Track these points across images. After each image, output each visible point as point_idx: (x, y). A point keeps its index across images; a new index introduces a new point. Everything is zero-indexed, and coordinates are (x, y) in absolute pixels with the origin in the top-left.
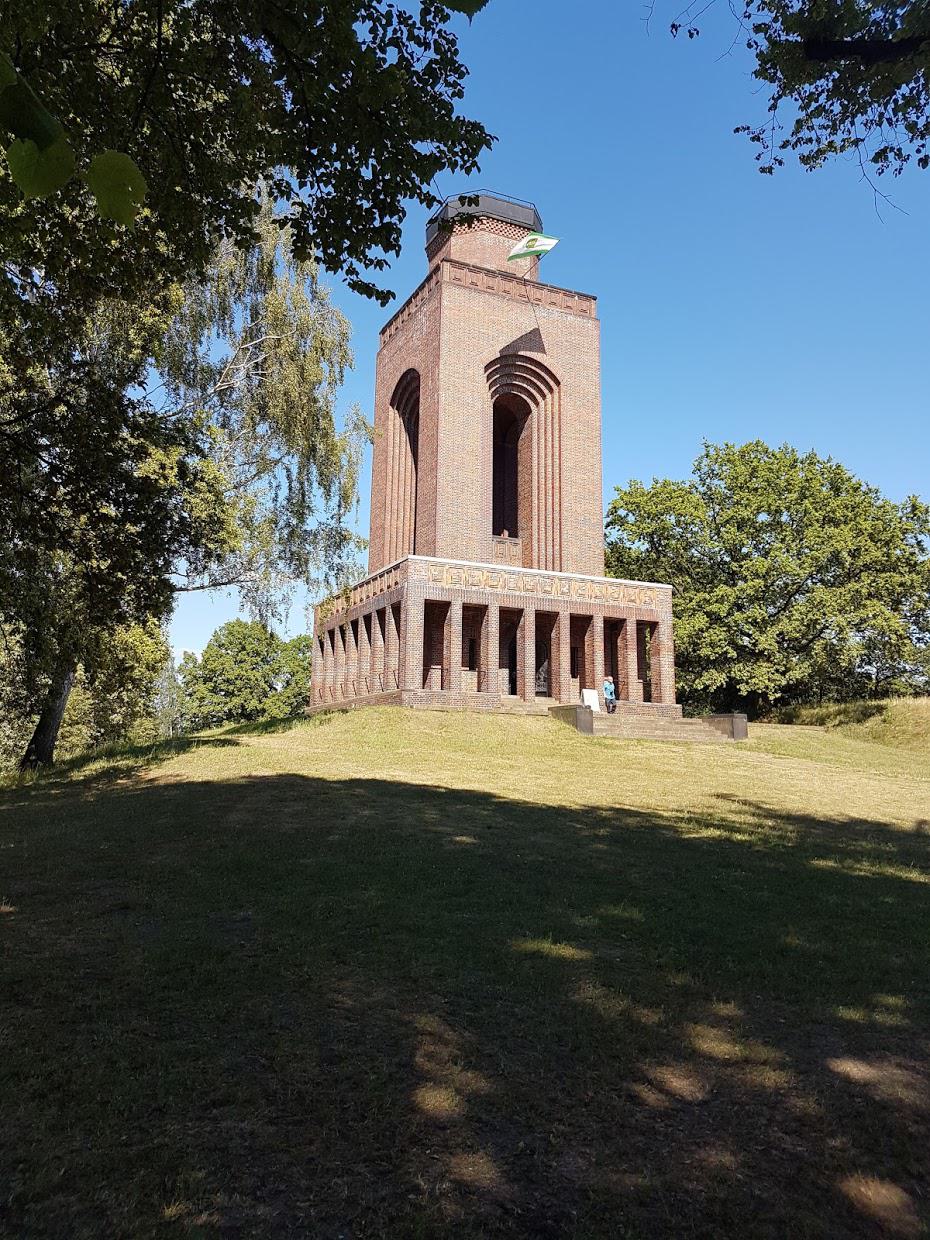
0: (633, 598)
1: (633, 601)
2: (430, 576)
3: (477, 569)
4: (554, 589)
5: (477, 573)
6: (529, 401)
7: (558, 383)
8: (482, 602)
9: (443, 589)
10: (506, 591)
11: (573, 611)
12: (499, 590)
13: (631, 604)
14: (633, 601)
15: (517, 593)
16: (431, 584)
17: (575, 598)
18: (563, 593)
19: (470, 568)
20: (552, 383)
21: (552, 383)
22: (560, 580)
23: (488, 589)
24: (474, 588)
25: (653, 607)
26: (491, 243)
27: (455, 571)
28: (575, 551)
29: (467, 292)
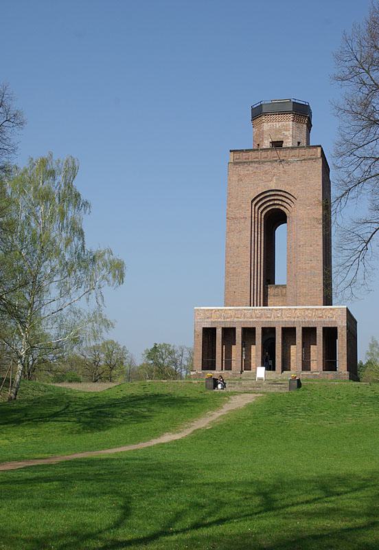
10: (246, 319)
13: (319, 319)
15: (251, 320)
18: (278, 317)
22: (276, 310)
24: (228, 320)
25: (334, 319)
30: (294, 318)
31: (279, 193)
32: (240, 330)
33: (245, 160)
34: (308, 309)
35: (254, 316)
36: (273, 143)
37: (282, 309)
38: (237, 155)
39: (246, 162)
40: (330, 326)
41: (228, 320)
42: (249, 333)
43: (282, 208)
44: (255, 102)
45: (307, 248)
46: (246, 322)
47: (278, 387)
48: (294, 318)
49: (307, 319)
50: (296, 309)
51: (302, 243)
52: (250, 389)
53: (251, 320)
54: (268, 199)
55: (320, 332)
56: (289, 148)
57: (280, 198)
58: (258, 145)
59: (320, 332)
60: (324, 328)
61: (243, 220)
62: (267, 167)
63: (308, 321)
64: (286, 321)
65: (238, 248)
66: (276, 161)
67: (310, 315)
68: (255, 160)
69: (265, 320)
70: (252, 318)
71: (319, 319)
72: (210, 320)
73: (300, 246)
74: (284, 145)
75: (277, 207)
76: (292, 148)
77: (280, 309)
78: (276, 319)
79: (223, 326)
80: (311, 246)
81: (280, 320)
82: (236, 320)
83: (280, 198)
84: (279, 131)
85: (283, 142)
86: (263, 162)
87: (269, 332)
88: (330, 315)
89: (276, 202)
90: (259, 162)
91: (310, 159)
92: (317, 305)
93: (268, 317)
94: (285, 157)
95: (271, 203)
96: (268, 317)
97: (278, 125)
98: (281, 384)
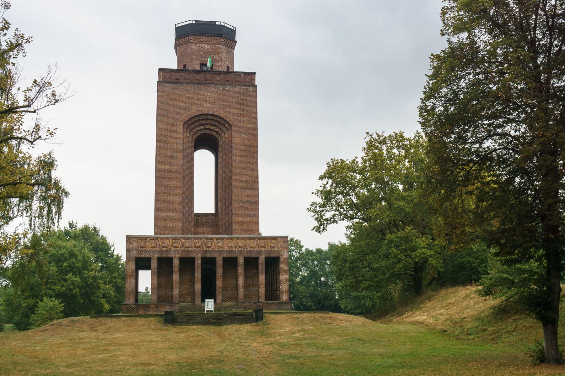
0: (263, 245)
1: (263, 247)
3: (167, 238)
5: (167, 242)
6: (217, 136)
7: (230, 125)
8: (168, 256)
9: (146, 251)
10: (183, 249)
11: (225, 256)
13: (261, 249)
14: (263, 247)
15: (190, 249)
16: (140, 249)
17: (226, 248)
18: (219, 246)
19: (162, 239)
21: (227, 126)
22: (217, 239)
23: (173, 248)
24: (164, 249)
25: (276, 249)
26: (196, 49)
27: (153, 241)
28: (240, 219)
29: (172, 85)
30: (236, 247)
31: (212, 118)
34: (250, 239)
35: (193, 244)
37: (223, 239)
40: (272, 256)
42: (187, 263)
43: (214, 134)
46: (184, 251)
48: (236, 247)
49: (249, 249)
55: (262, 262)
56: (223, 72)
59: (262, 262)
63: (250, 251)
64: (227, 251)
67: (252, 245)
69: (205, 249)
70: (192, 247)
71: (261, 249)
72: (144, 249)
75: (208, 132)
76: (196, 71)
77: (221, 238)
78: (217, 249)
81: (221, 249)
82: (173, 249)
87: (209, 263)
88: (272, 245)
89: (208, 127)
93: (208, 247)
96: (208, 247)
97: (207, 47)
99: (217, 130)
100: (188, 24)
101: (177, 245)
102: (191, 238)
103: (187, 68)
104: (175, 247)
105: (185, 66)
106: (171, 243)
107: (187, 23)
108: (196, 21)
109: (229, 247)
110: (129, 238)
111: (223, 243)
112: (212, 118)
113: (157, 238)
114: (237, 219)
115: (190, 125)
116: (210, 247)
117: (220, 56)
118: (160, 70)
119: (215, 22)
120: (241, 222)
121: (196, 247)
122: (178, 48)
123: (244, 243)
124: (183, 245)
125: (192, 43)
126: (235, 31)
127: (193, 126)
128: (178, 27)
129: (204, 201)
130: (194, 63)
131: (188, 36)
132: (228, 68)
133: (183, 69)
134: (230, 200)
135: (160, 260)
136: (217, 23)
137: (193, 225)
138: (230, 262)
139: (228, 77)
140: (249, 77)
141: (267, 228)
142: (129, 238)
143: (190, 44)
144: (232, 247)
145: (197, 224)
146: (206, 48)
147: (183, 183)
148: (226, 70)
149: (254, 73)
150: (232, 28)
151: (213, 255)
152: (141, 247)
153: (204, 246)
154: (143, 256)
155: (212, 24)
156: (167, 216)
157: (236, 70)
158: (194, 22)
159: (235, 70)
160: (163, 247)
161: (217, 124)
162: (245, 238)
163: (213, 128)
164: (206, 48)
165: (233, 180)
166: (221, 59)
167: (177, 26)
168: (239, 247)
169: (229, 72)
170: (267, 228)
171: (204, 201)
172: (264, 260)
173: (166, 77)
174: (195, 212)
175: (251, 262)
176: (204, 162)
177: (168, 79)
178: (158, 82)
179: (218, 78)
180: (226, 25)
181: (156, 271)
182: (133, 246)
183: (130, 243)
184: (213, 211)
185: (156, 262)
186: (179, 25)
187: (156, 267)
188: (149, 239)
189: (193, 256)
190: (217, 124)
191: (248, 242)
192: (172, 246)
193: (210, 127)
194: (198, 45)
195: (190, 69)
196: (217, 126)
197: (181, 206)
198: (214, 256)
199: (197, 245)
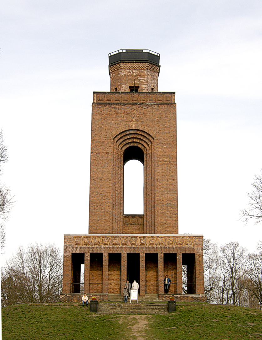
0: (180, 243)
2: (74, 242)
4: (137, 242)
5: (97, 239)
7: (153, 139)
8: (99, 252)
10: (112, 246)
11: (147, 252)
12: (108, 246)
13: (179, 246)
14: (181, 244)
15: (118, 246)
16: (75, 246)
17: (148, 246)
18: (142, 244)
20: (151, 139)
21: (151, 139)
22: (140, 237)
24: (95, 246)
27: (86, 239)
30: (156, 245)
31: (138, 132)
32: (107, 255)
33: (107, 102)
34: (169, 237)
36: (130, 87)
38: (101, 97)
39: (109, 104)
41: (95, 246)
42: (115, 259)
43: (140, 146)
44: (114, 50)
45: (164, 182)
47: (156, 309)
48: (156, 245)
49: (168, 246)
50: (158, 237)
51: (159, 178)
52: (132, 310)
53: (118, 246)
54: (128, 137)
56: (147, 93)
57: (139, 137)
58: (116, 89)
60: (183, 254)
61: (106, 155)
62: (128, 108)
64: (149, 248)
65: (101, 180)
66: (136, 103)
67: (171, 242)
68: (117, 102)
70: (118, 244)
71: (179, 246)
72: (78, 246)
73: (157, 180)
74: (140, 90)
75: (135, 145)
77: (143, 237)
79: (91, 252)
80: (167, 180)
81: (143, 246)
82: (103, 246)
83: (139, 137)
84: (136, 77)
85: (138, 87)
86: (124, 104)
87: (133, 258)
88: (188, 243)
90: (120, 104)
91: (166, 104)
92: (173, 233)
93: (133, 244)
94: (143, 100)
95: (131, 141)
96: (133, 244)
98: (158, 306)
99: (142, 142)
100: (119, 53)
101: (106, 242)
102: (118, 236)
103: (118, 91)
104: (105, 244)
105: (116, 89)
106: (101, 240)
107: (117, 52)
108: (126, 50)
109: (151, 244)
110: (66, 237)
111: (145, 240)
112: (138, 132)
113: (89, 236)
114: (160, 220)
115: (119, 139)
116: (135, 244)
117: (146, 79)
118: (94, 93)
119: (143, 50)
120: (163, 222)
121: (123, 244)
122: (111, 74)
123: (164, 241)
124: (111, 243)
125: (121, 69)
126: (159, 57)
127: (121, 140)
128: (111, 56)
129: (134, 203)
130: (124, 86)
131: (119, 63)
132: (152, 89)
133: (115, 91)
134: (153, 202)
135: (93, 255)
136: (144, 51)
137: (121, 224)
138: (152, 259)
139: (153, 97)
140: (170, 96)
141: (186, 227)
142: (66, 237)
143: (120, 71)
144: (153, 244)
145: (125, 224)
146: (134, 73)
147: (113, 189)
148: (150, 91)
149: (174, 93)
150: (157, 54)
151: (69, 256)
152: (76, 244)
153: (129, 243)
154: (78, 252)
155: (140, 52)
156: (99, 217)
157: (160, 90)
158: (125, 51)
159: (159, 91)
160: (95, 244)
161: (142, 138)
162: (165, 237)
163: (139, 141)
164: (134, 73)
165: (156, 186)
166: (147, 82)
167: (110, 55)
168: (160, 244)
169: (153, 92)
170: (186, 227)
171: (134, 203)
172: (181, 256)
173: (101, 100)
174: (125, 213)
175: (170, 259)
176: (134, 170)
177: (101, 100)
178: (92, 103)
179: (143, 99)
180: (151, 52)
181: (89, 265)
182: (69, 243)
183: (67, 240)
184: (143, 214)
185: (89, 257)
186: (112, 54)
187: (89, 261)
188: (83, 237)
189: (120, 252)
190: (142, 138)
191: (168, 240)
192: (102, 243)
193: (136, 141)
194: (127, 70)
195: (120, 91)
196: (142, 140)
197: (111, 209)
198: (137, 252)
199: (123, 242)
